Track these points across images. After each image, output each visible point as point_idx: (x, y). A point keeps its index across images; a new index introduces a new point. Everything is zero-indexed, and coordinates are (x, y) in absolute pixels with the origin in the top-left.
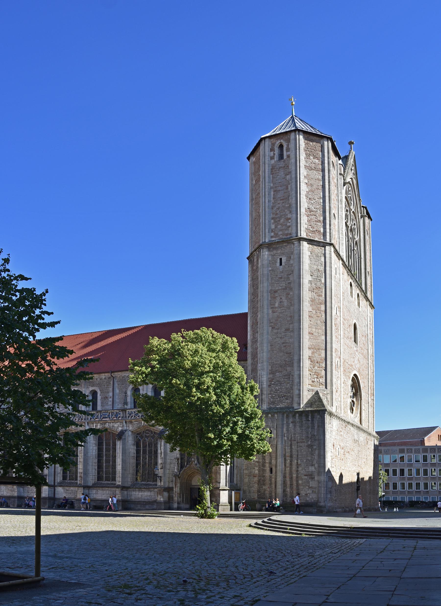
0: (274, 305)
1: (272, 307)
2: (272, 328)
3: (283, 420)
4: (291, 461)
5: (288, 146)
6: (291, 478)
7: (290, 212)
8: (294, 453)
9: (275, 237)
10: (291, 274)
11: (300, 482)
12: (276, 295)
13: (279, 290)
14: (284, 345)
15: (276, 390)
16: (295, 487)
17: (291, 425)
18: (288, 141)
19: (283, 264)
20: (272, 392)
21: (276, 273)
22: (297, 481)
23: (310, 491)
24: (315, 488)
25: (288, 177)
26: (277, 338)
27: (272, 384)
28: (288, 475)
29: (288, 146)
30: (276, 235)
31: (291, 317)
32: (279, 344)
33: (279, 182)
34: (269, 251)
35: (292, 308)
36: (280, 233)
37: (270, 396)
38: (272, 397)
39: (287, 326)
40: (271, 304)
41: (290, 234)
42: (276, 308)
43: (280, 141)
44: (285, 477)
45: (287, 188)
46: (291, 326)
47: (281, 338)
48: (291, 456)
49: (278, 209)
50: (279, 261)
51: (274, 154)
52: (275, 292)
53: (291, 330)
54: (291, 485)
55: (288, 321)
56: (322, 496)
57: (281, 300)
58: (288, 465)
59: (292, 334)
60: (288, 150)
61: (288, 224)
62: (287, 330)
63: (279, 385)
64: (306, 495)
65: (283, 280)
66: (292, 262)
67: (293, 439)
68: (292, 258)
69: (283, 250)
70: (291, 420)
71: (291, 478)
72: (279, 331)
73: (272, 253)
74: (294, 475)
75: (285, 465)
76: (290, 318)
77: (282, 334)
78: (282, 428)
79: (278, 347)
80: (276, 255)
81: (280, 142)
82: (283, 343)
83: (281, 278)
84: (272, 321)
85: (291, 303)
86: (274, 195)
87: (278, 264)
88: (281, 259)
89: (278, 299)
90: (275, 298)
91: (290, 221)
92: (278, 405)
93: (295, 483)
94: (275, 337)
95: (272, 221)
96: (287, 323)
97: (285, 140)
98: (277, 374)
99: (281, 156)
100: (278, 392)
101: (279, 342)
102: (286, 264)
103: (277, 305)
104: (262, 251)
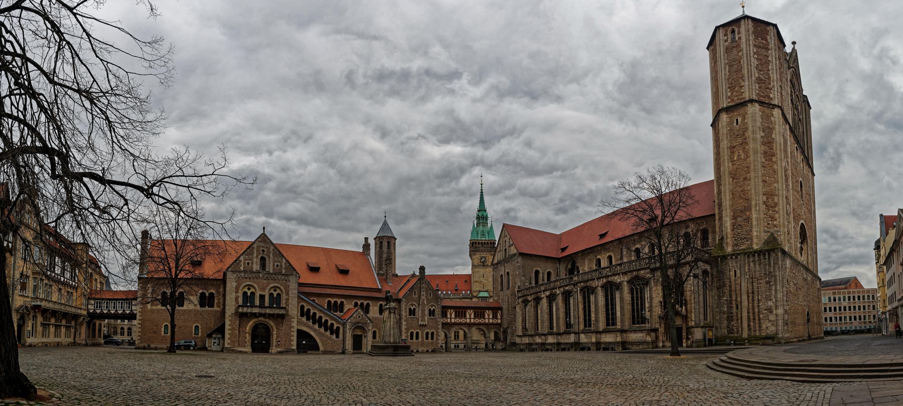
3: (745, 261)
4: (753, 297)
6: (754, 313)
7: (743, 80)
8: (756, 290)
11: (761, 316)
16: (757, 322)
17: (752, 264)
19: (739, 123)
22: (759, 315)
23: (769, 325)
24: (774, 321)
28: (751, 311)
30: (732, 100)
31: (747, 167)
34: (727, 114)
36: (736, 98)
41: (744, 98)
42: (735, 161)
44: (748, 312)
48: (753, 293)
50: (735, 122)
52: (734, 147)
54: (754, 319)
56: (780, 328)
58: (750, 301)
61: (742, 91)
64: (767, 328)
66: (746, 121)
67: (754, 276)
70: (751, 259)
71: (754, 313)
74: (756, 310)
75: (748, 302)
78: (745, 267)
82: (742, 191)
83: (738, 135)
85: (747, 155)
87: (735, 124)
88: (737, 120)
93: (757, 317)
95: (729, 90)
103: (735, 158)
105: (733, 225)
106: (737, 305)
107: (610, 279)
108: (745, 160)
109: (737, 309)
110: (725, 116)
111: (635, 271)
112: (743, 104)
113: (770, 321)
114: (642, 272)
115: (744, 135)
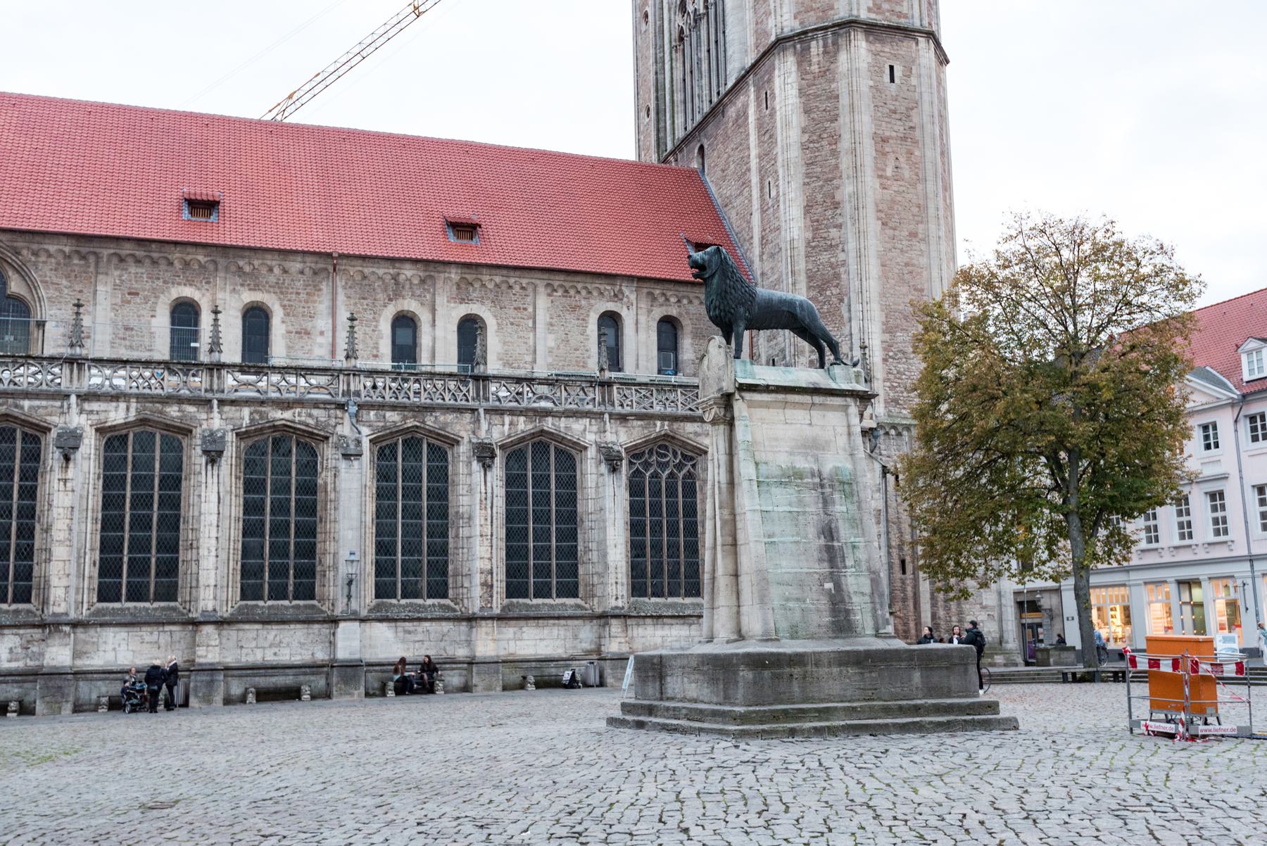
0: (884, 170)
1: (880, 173)
2: (883, 224)
9: (877, 14)
10: (912, 109)
12: (887, 149)
13: (891, 137)
14: (910, 268)
19: (896, 80)
20: (891, 377)
21: (883, 96)
27: (891, 357)
31: (919, 206)
32: (898, 264)
35: (920, 187)
37: (888, 384)
38: (892, 388)
39: (912, 226)
40: (878, 169)
41: (906, 16)
42: (887, 178)
46: (921, 227)
47: (902, 250)
50: (887, 71)
52: (885, 140)
53: (920, 236)
55: (913, 215)
57: (897, 164)
59: (923, 247)
62: (913, 235)
65: (898, 116)
66: (914, 81)
68: (914, 71)
72: (897, 233)
73: (873, 48)
82: (907, 265)
85: (917, 175)
87: (887, 78)
88: (892, 68)
89: (891, 157)
90: (885, 154)
94: (889, 246)
101: (899, 260)
103: (889, 172)
104: (852, 37)
105: (887, 347)
106: (903, 562)
107: (549, 424)
108: (914, 185)
109: (904, 572)
111: (663, 418)
112: (906, 32)
113: (984, 608)
114: (690, 427)
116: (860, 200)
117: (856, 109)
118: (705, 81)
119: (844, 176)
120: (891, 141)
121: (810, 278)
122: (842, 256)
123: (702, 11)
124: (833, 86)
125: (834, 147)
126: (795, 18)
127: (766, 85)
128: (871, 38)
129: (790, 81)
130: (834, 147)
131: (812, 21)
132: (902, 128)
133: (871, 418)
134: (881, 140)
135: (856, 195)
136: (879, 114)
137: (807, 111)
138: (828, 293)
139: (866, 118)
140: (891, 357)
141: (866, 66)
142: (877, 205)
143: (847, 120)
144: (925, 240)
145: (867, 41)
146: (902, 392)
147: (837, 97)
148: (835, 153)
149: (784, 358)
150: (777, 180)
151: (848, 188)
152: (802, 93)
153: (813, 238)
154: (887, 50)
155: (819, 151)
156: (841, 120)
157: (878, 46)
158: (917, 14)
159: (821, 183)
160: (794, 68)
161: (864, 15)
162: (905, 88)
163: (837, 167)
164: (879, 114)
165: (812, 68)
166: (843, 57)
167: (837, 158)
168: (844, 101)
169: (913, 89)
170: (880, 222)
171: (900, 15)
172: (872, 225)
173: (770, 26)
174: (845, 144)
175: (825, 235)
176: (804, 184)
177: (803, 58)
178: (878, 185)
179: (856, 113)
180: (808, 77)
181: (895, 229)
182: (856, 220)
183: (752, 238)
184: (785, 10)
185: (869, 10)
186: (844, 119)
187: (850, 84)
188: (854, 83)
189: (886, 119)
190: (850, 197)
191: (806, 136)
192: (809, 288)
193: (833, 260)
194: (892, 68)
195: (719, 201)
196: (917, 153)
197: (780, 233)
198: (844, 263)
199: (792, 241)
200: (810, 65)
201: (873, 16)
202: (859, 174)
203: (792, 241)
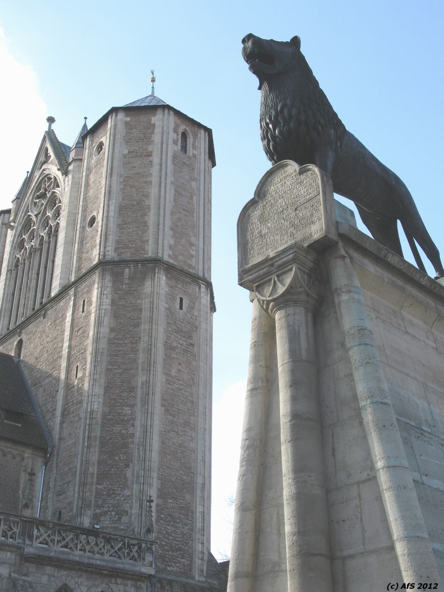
1: (167, 372)
2: (166, 410)
5: (194, 142)
12: (173, 356)
15: (167, 533)
18: (195, 136)
20: (161, 536)
25: (194, 184)
26: (171, 432)
29: (194, 142)
32: (174, 444)
33: (182, 183)
36: (181, 258)
41: (193, 268)
42: (171, 376)
43: (185, 127)
45: (192, 199)
46: (192, 418)
49: (180, 219)
50: (178, 301)
51: (177, 138)
52: (173, 348)
55: (188, 409)
57: (180, 368)
60: (194, 147)
63: (172, 523)
69: (185, 287)
72: (175, 419)
76: (191, 405)
77: (179, 428)
79: (172, 449)
80: (175, 288)
81: (185, 129)
84: (165, 397)
86: (175, 195)
87: (178, 306)
88: (181, 299)
91: (194, 248)
92: (169, 566)
96: (186, 410)
97: (193, 133)
98: (170, 501)
99: (184, 148)
100: (171, 537)
101: (175, 441)
102: (188, 311)
104: (157, 271)
110: (164, 278)
115: (190, 337)
116: (151, 388)
117: (154, 321)
118: (32, 294)
119: (140, 368)
120: (177, 350)
121: (102, 445)
122: (131, 430)
123: (37, 246)
124: (138, 302)
125: (135, 346)
126: (115, 251)
127: (85, 296)
128: (169, 275)
129: (105, 292)
130: (135, 346)
131: (127, 256)
132: (185, 343)
133: (151, 566)
134: (169, 347)
135: (147, 384)
136: (170, 329)
137: (116, 316)
138: (116, 458)
139: (161, 329)
140: (162, 519)
141: (164, 293)
142: (163, 396)
143: (147, 327)
144: (194, 429)
145: (166, 276)
146: (168, 551)
147: (141, 310)
148: (135, 351)
149: (72, 509)
150: (85, 364)
151: (141, 379)
152: (113, 303)
153: (109, 412)
154: (179, 286)
155: (122, 346)
156: (142, 327)
157: (173, 283)
158: (201, 268)
159: (121, 371)
160: (110, 284)
161: (166, 258)
162: (189, 316)
163: (135, 361)
164: (170, 329)
165: (124, 286)
166: (148, 283)
167: (136, 354)
168: (146, 314)
169: (194, 318)
170: (163, 408)
171: (190, 266)
172: (158, 409)
173: (94, 255)
174: (142, 345)
175: (120, 411)
176: (107, 369)
177: (117, 278)
178: (164, 380)
179: (154, 324)
180: (119, 292)
181: (173, 416)
182: (145, 402)
183: (55, 410)
184: (108, 244)
185: (170, 256)
186: (144, 326)
187: (152, 303)
188: (155, 303)
189: (174, 334)
190: (143, 384)
191: (113, 334)
192: (101, 452)
193: (123, 431)
194: (181, 299)
195: (29, 382)
196: (194, 363)
197: (82, 405)
198: (133, 435)
199: (92, 412)
200: (122, 285)
201: (171, 261)
202: (152, 368)
203: (92, 412)
